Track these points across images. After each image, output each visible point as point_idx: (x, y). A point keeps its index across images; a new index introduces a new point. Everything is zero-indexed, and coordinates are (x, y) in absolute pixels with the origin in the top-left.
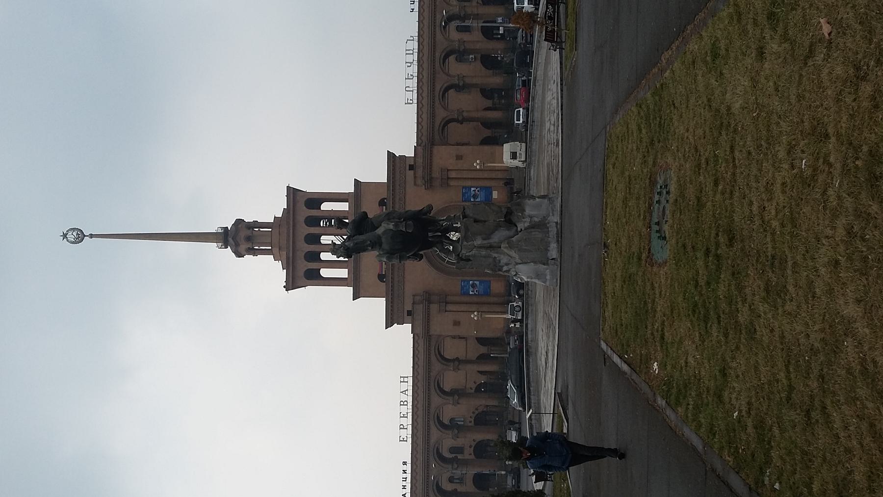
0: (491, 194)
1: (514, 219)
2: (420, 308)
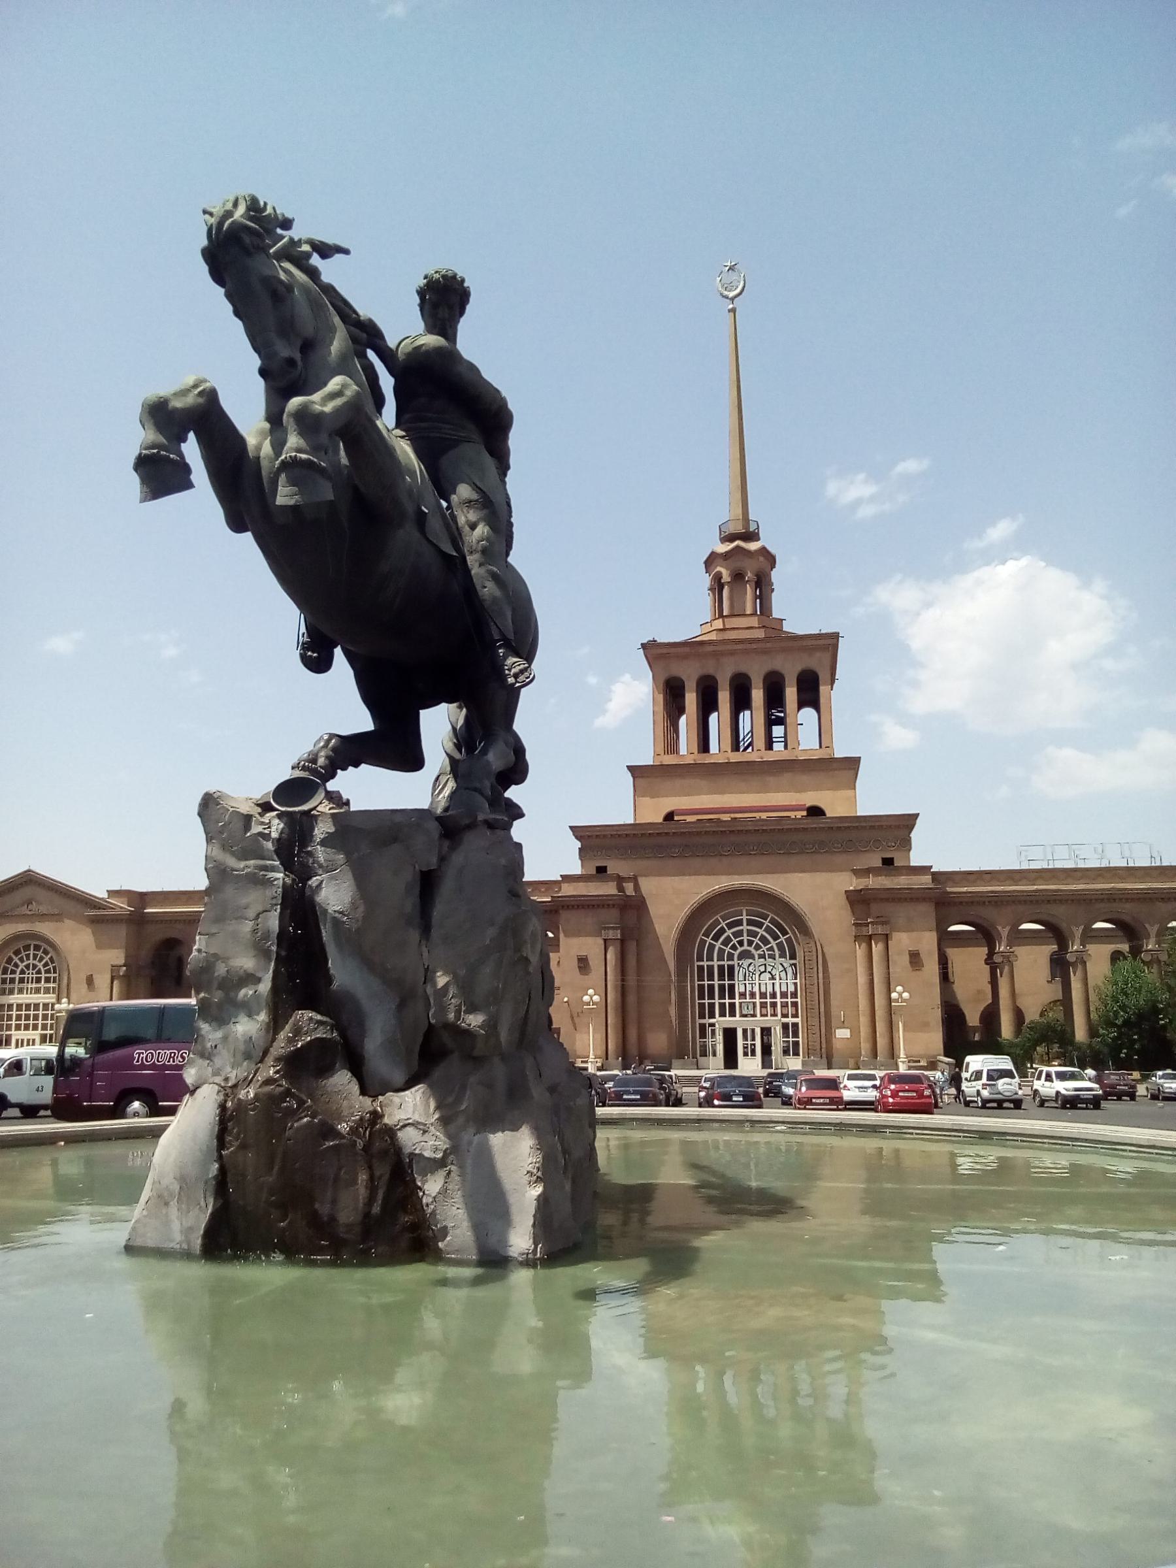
0: (843, 1026)
1: (438, 1073)
2: (608, 889)
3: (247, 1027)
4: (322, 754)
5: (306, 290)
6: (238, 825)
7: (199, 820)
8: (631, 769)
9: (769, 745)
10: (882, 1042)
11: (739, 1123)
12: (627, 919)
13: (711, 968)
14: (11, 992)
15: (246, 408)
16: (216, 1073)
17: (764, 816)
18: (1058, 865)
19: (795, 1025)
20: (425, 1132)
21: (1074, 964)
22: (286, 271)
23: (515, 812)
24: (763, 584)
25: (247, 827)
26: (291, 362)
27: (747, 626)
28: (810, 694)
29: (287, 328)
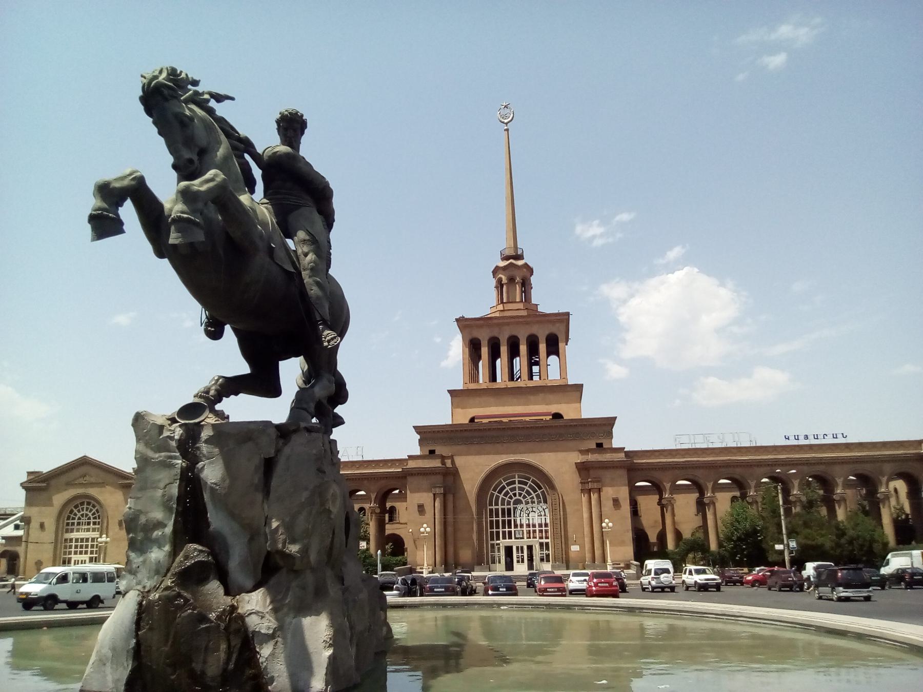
0: (575, 543)
1: (273, 581)
2: (436, 463)
3: (157, 555)
4: (214, 388)
5: (202, 120)
6: (155, 432)
7: (132, 429)
8: (449, 391)
9: (531, 377)
10: (598, 553)
11: (490, 605)
12: (447, 481)
13: (497, 510)
14: (72, 531)
15: (166, 187)
16: (138, 583)
17: (527, 419)
18: (698, 446)
19: (547, 544)
20: (262, 617)
21: (708, 504)
22: (190, 109)
23: (339, 421)
24: (526, 285)
25: (161, 433)
26: (191, 161)
27: (517, 308)
28: (554, 348)
29: (189, 141)
